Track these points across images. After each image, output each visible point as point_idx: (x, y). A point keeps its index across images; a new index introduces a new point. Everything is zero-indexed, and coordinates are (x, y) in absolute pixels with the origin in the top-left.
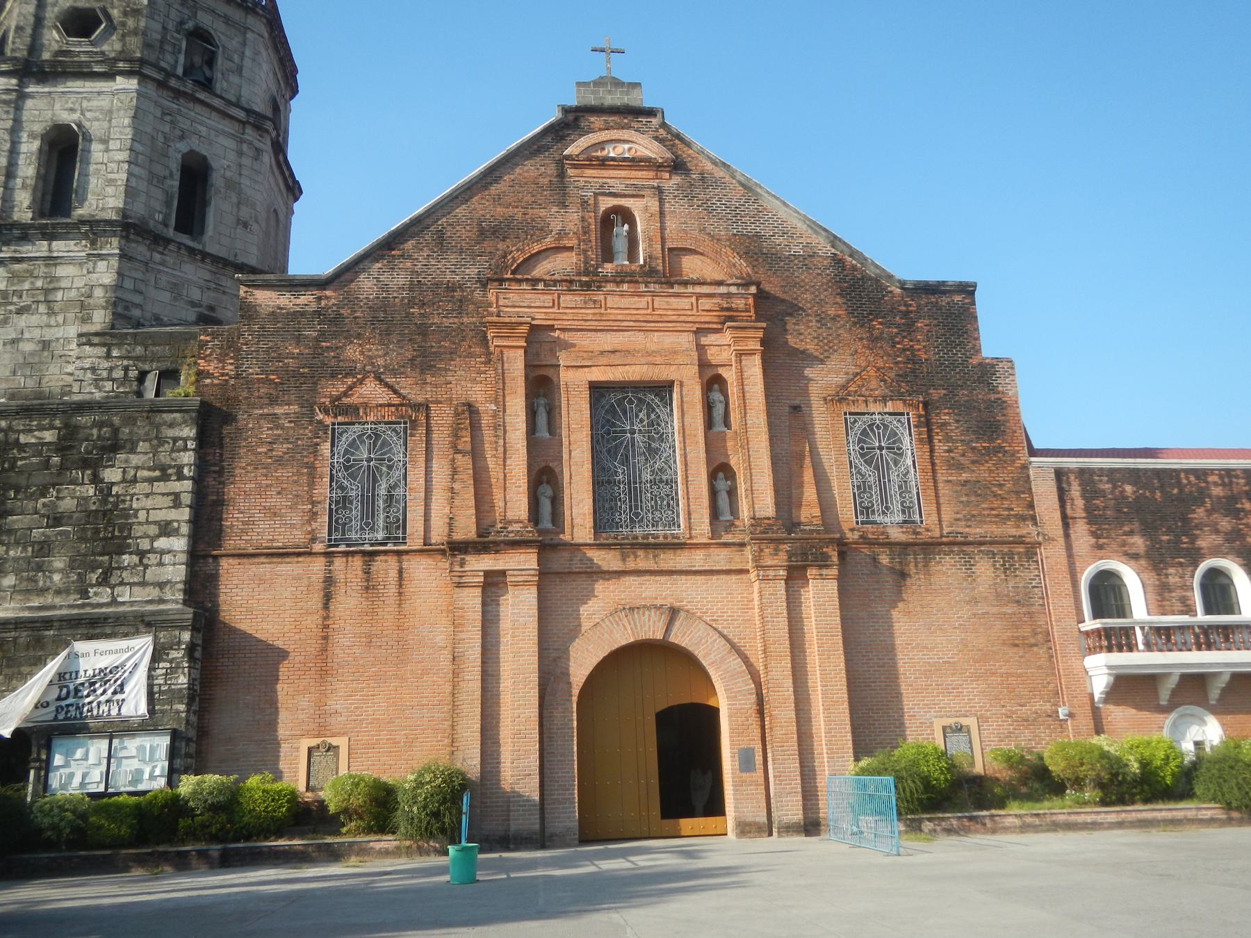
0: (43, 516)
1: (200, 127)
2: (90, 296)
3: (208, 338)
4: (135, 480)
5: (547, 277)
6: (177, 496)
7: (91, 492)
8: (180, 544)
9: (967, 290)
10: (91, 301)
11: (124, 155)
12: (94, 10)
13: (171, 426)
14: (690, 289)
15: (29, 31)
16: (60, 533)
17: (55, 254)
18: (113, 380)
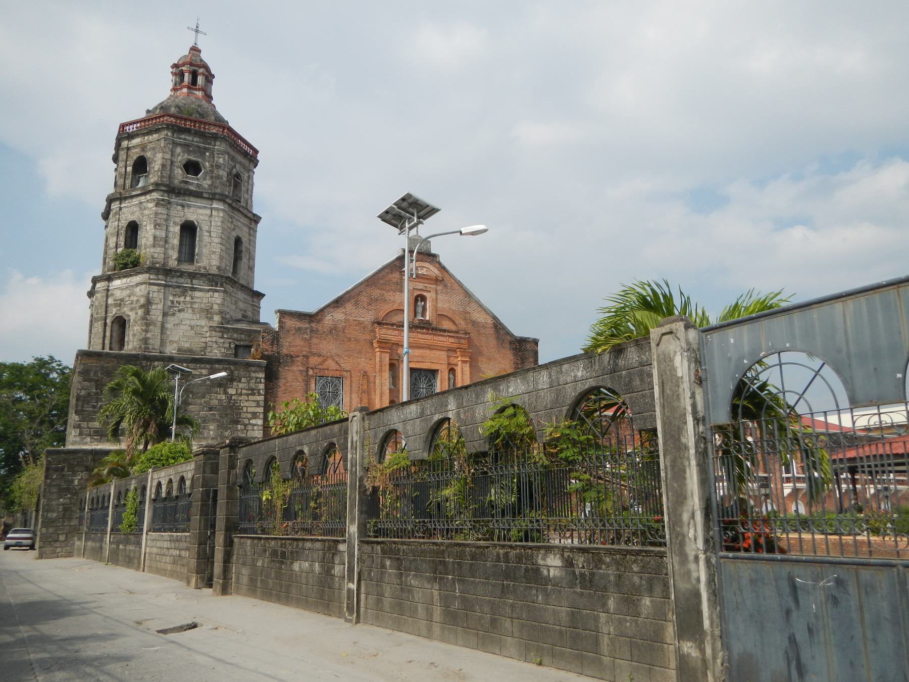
0: (204, 407)
1: (239, 224)
2: (212, 308)
3: (266, 335)
4: (241, 394)
5: (398, 324)
6: (258, 402)
7: (224, 398)
8: (260, 422)
9: (536, 342)
10: (213, 310)
11: (218, 240)
12: (198, 162)
13: (254, 372)
14: (446, 334)
15: (168, 167)
16: (212, 414)
17: (195, 286)
18: (225, 348)
